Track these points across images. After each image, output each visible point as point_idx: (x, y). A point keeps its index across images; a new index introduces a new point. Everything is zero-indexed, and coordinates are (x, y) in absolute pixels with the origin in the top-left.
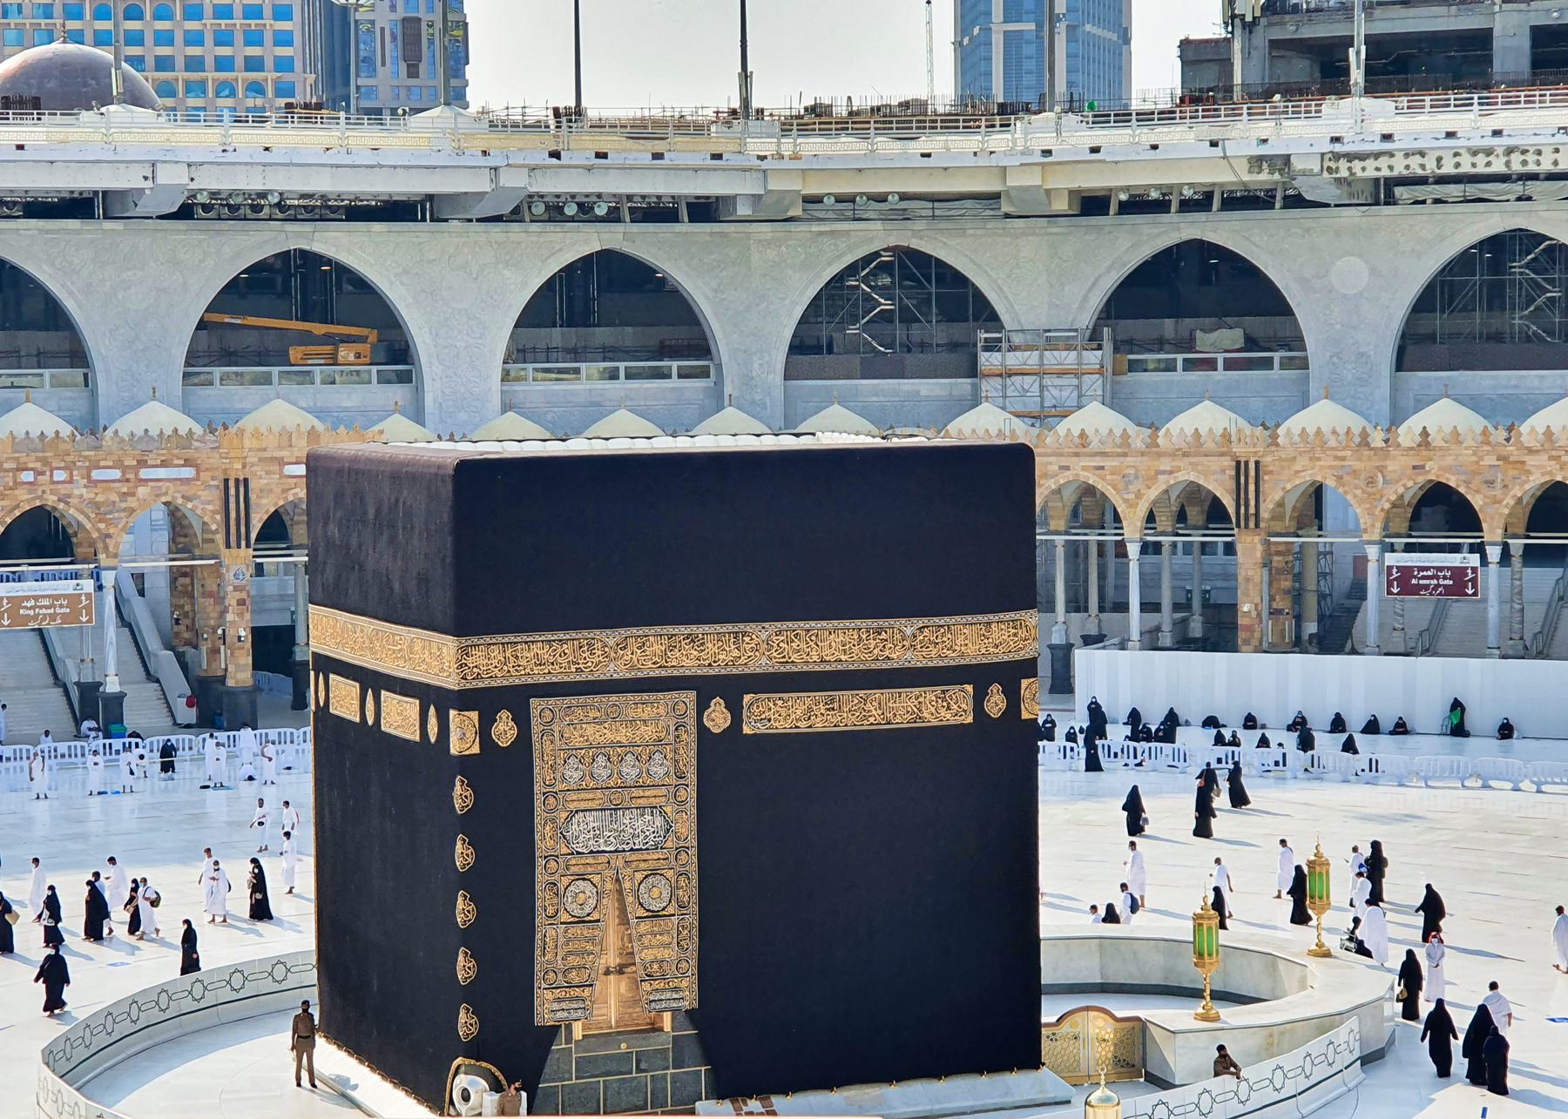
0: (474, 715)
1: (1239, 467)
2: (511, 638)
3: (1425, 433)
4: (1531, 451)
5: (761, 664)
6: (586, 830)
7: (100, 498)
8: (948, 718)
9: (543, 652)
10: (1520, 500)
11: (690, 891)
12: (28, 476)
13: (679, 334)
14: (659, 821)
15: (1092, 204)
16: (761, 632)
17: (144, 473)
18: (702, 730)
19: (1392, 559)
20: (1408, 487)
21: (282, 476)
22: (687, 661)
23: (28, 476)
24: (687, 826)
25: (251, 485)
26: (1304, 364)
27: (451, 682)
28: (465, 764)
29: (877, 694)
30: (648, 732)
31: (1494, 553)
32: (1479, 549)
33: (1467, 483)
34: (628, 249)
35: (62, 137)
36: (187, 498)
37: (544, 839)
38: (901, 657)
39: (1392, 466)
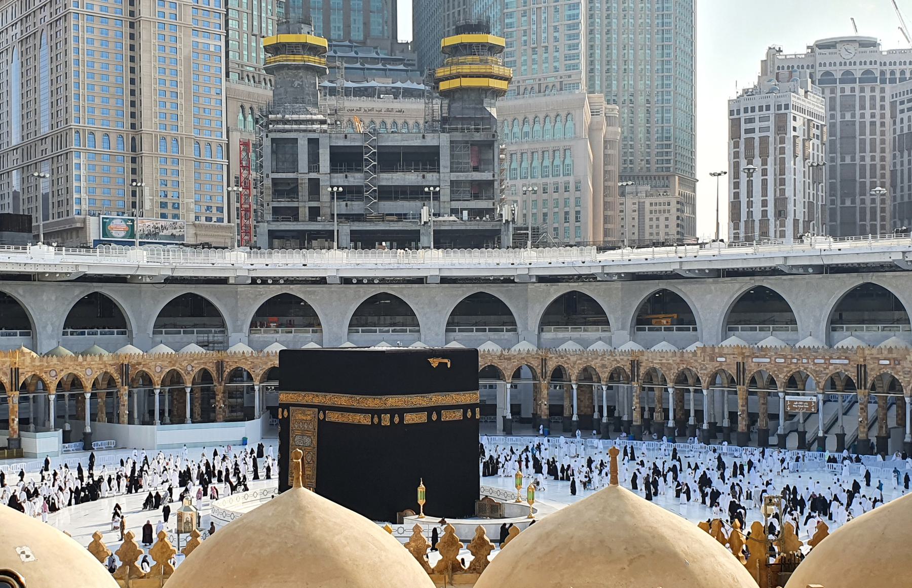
5: (329, 403)
7: (817, 369)
8: (365, 422)
11: (315, 459)
12: (795, 361)
13: (505, 318)
16: (329, 395)
17: (832, 361)
21: (879, 364)
22: (316, 401)
23: (795, 361)
24: (315, 442)
25: (869, 367)
30: (309, 418)
35: (855, 245)
36: (846, 371)
37: (291, 442)
38: (356, 405)
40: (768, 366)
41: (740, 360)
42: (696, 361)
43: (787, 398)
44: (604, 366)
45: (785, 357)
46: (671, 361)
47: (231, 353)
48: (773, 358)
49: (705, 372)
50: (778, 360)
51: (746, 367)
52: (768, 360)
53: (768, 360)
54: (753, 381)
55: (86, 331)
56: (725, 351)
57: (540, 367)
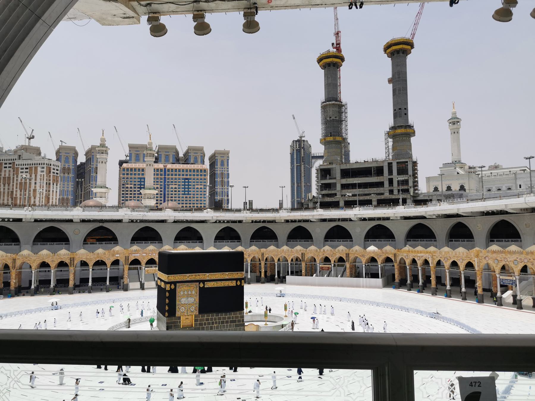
0: (169, 285)
1: (302, 254)
2: (175, 275)
3: (324, 250)
4: (337, 252)
6: (184, 301)
8: (232, 285)
9: (179, 277)
10: (336, 258)
12: (150, 254)
14: (194, 299)
15: (287, 221)
16: (207, 274)
18: (199, 287)
19: (320, 266)
20: (324, 256)
23: (150, 254)
26: (313, 241)
27: (167, 281)
28: (168, 291)
29: (223, 282)
31: (333, 265)
32: (331, 265)
33: (329, 256)
34: (230, 226)
38: (227, 277)
39: (320, 254)
40: (139, 257)
41: (127, 255)
42: (105, 257)
43: (146, 269)
44: (53, 261)
45: (146, 253)
46: (92, 257)
47: (368, 250)
48: (141, 254)
49: (110, 261)
50: (143, 255)
51: (129, 258)
52: (139, 255)
53: (139, 255)
54: (266, 259)
55: (370, 240)
56: (120, 252)
57: (12, 263)
